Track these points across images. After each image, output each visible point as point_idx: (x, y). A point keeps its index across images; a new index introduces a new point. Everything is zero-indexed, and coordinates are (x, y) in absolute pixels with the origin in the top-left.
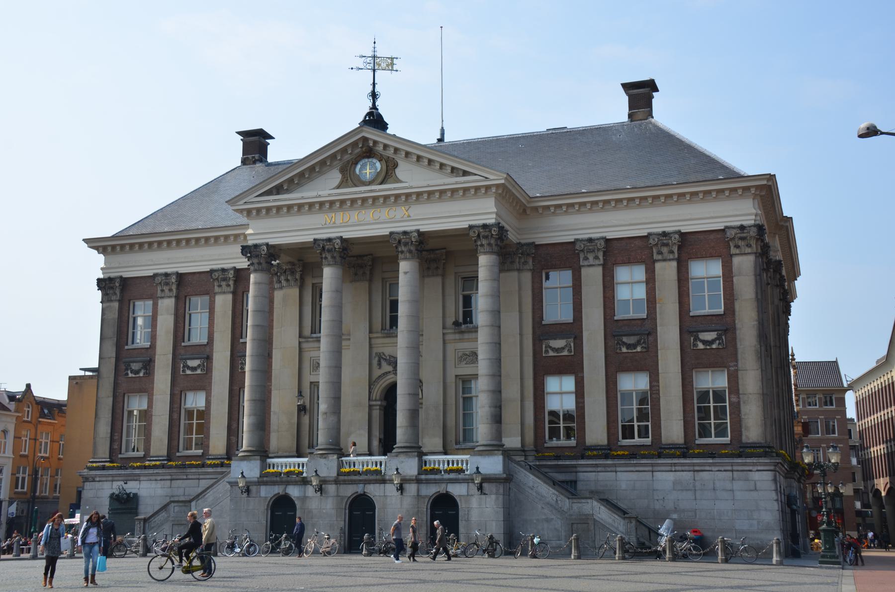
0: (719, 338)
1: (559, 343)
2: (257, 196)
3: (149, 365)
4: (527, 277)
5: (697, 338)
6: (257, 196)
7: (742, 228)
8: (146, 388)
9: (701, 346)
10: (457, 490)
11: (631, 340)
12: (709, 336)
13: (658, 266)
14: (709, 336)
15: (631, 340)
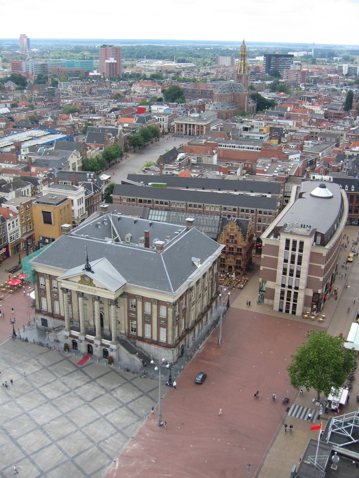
0: (165, 323)
1: (133, 314)
2: (63, 279)
3: (45, 292)
4: (126, 299)
5: (160, 322)
6: (63, 279)
7: (170, 303)
8: (45, 296)
9: (161, 323)
10: (108, 349)
11: (148, 318)
12: (163, 322)
13: (153, 305)
14: (163, 322)
15: (148, 318)
